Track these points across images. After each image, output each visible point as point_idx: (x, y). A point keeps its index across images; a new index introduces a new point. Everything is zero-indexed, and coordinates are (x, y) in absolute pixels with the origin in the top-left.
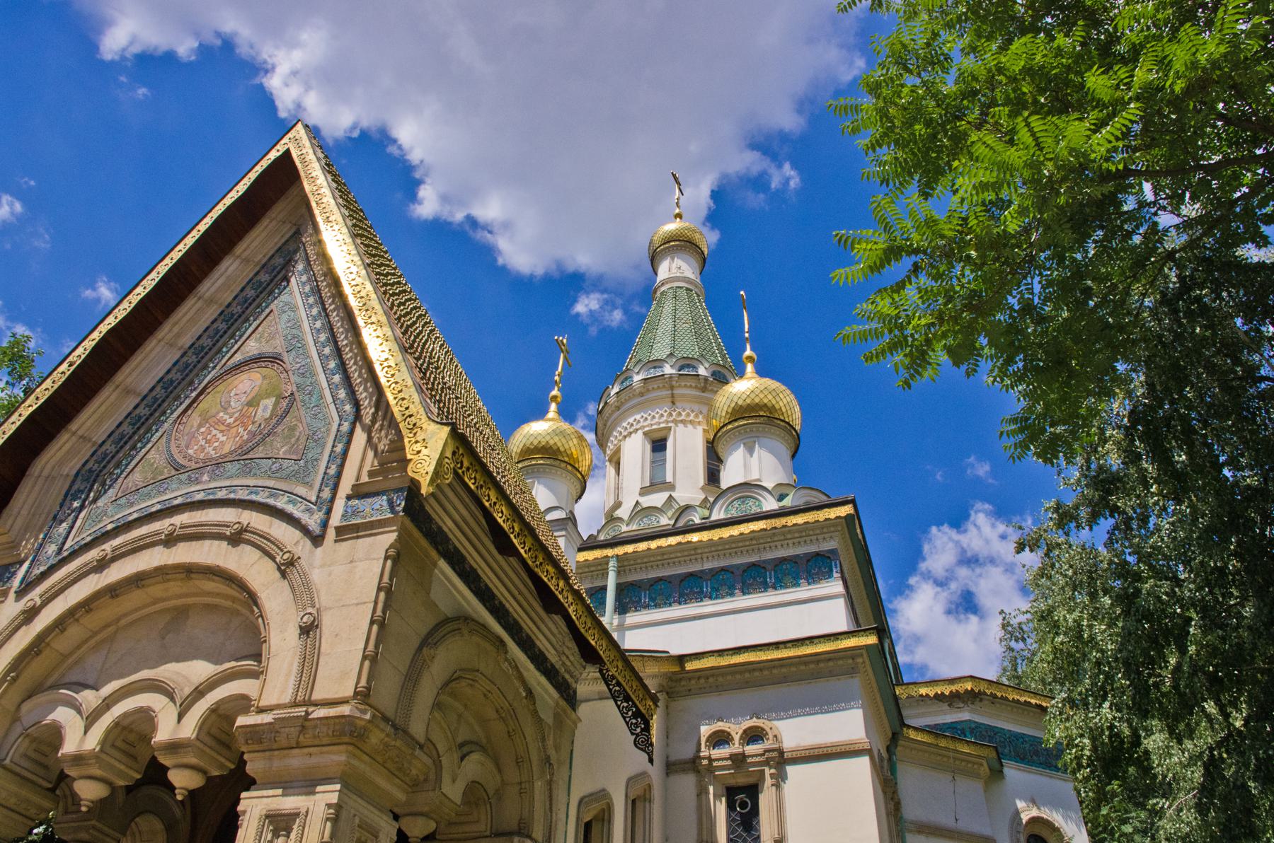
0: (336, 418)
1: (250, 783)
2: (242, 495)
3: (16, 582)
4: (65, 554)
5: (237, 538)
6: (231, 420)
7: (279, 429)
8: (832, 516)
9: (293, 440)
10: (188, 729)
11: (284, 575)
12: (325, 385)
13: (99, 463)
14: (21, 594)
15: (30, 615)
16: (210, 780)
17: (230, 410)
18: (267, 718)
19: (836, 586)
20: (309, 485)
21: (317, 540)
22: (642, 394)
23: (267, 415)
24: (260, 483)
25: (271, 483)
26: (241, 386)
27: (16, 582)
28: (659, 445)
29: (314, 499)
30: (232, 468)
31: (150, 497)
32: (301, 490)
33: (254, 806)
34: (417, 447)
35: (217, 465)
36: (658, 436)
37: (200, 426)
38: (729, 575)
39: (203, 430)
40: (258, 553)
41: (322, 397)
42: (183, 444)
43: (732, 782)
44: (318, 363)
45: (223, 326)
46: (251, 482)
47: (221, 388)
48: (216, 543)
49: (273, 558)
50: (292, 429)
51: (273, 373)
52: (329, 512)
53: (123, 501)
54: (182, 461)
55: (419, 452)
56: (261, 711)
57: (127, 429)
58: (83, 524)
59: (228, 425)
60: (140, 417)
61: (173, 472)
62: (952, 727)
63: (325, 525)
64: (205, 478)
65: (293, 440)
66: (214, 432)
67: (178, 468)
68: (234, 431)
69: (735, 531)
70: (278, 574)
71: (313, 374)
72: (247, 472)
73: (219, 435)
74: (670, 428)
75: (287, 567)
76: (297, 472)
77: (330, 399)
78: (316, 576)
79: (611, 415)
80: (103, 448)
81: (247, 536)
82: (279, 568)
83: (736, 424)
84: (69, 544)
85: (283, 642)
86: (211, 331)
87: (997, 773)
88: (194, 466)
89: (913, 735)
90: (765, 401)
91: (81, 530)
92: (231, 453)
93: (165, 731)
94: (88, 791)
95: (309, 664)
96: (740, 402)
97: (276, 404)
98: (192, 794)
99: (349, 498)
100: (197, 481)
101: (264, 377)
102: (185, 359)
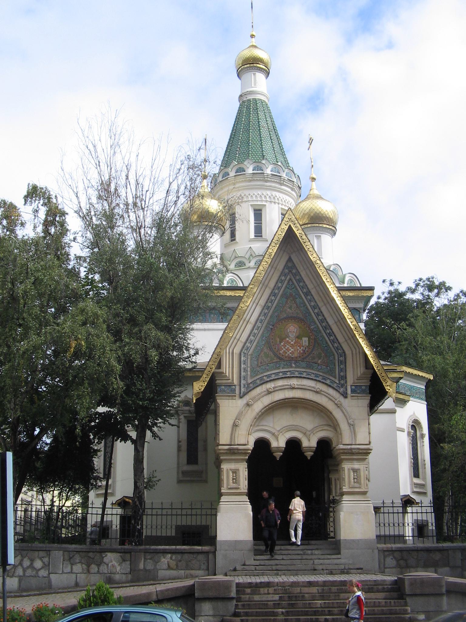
0: (336, 354)
2: (312, 376)
3: (237, 392)
6: (292, 343)
8: (365, 295)
9: (322, 358)
10: (313, 443)
14: (241, 397)
18: (349, 447)
20: (335, 377)
22: (250, 181)
23: (307, 344)
25: (321, 374)
26: (290, 328)
27: (237, 392)
28: (258, 214)
29: (338, 382)
30: (304, 364)
31: (275, 369)
32: (333, 379)
37: (280, 342)
39: (282, 344)
41: (327, 343)
44: (321, 328)
48: (311, 393)
49: (334, 402)
56: (344, 445)
57: (252, 338)
60: (255, 334)
61: (278, 360)
63: (347, 393)
65: (322, 358)
67: (281, 359)
71: (320, 332)
72: (309, 366)
74: (265, 205)
75: (338, 406)
78: (349, 409)
81: (322, 393)
82: (336, 404)
85: (344, 426)
91: (252, 377)
92: (300, 357)
97: (309, 341)
99: (351, 386)
100: (292, 367)
101: (300, 327)
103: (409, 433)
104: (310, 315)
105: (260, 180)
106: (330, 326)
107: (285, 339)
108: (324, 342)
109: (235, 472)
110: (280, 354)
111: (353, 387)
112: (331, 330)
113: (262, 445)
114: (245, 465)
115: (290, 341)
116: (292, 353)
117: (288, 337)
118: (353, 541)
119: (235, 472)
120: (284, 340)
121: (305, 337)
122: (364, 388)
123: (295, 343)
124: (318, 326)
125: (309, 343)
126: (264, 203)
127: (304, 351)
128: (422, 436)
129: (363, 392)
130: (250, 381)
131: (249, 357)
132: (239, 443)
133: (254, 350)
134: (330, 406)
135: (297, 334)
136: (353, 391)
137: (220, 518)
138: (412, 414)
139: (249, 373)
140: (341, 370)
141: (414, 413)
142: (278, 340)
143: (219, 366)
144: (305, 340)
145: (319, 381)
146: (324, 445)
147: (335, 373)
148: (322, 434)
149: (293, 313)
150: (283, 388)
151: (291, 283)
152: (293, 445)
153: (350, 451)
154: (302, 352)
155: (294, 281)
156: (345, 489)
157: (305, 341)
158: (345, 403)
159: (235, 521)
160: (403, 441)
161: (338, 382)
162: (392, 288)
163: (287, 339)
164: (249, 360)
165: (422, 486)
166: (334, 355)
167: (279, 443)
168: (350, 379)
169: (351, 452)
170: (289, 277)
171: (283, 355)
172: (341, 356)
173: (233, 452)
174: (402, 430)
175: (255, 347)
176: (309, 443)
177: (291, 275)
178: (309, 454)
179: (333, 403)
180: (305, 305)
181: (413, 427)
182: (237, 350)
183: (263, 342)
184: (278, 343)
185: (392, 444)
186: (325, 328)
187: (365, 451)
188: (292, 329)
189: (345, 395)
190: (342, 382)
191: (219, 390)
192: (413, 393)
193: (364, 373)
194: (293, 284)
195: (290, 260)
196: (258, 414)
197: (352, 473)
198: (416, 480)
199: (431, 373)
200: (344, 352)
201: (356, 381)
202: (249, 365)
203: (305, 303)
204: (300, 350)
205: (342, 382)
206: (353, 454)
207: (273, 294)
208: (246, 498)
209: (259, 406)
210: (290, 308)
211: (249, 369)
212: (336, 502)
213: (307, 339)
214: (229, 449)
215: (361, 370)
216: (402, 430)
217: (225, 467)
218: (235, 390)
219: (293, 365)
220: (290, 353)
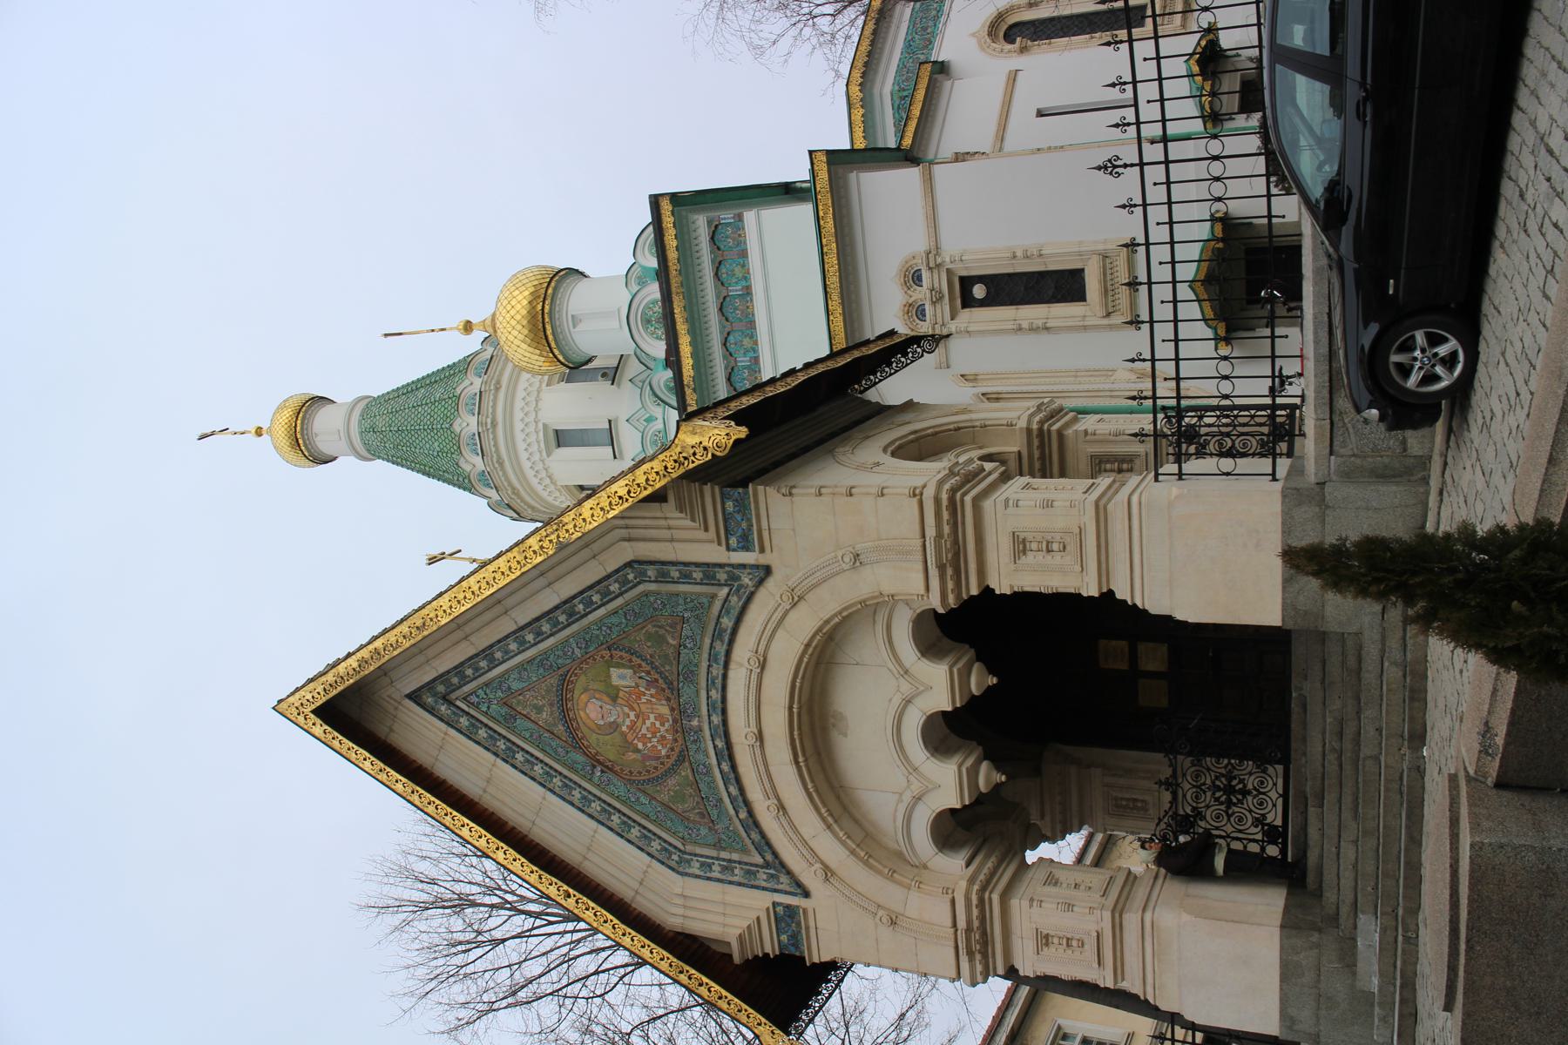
0: (641, 588)
1: (987, 591)
2: (717, 671)
4: (769, 857)
6: (632, 715)
7: (648, 652)
9: (662, 632)
11: (801, 598)
12: (602, 612)
13: (671, 854)
14: (807, 894)
15: (828, 873)
16: (978, 659)
17: (620, 720)
19: (750, 216)
20: (714, 596)
21: (768, 570)
23: (629, 672)
24: (705, 656)
25: (707, 641)
26: (593, 715)
28: (561, 438)
29: (726, 590)
30: (687, 691)
31: (714, 781)
33: (1004, 581)
34: (700, 451)
35: (681, 714)
36: (552, 436)
38: (731, 338)
39: (640, 746)
40: (780, 633)
42: (654, 763)
43: (959, 302)
44: (575, 627)
45: (519, 756)
46: (705, 664)
47: (593, 738)
50: (649, 636)
51: (583, 678)
52: (744, 566)
53: (714, 813)
54: (674, 758)
55: (705, 449)
57: (635, 832)
58: (736, 851)
59: (637, 716)
62: (896, 109)
63: (757, 567)
64: (695, 723)
65: (662, 632)
66: (644, 731)
67: (682, 758)
68: (643, 708)
69: (682, 328)
70: (802, 605)
71: (587, 629)
72: (690, 676)
73: (648, 723)
74: (545, 426)
76: (697, 617)
77: (620, 601)
79: (523, 500)
80: (656, 854)
81: (761, 649)
83: (551, 338)
84: (759, 860)
86: (526, 768)
87: (942, 68)
88: (681, 741)
89: (907, 142)
90: (525, 302)
91: (744, 851)
92: (668, 699)
94: (988, 776)
96: (526, 332)
97: (618, 666)
98: (992, 671)
99: (728, 548)
101: (586, 690)
102: (557, 790)
103: (1023, 50)
104: (545, 654)
105: (495, 438)
106: (565, 602)
107: (624, 735)
108: (614, 620)
109: (1044, 940)
110: (668, 757)
111: (733, 541)
112: (574, 597)
113: (955, 829)
115: (628, 722)
116: (659, 717)
117: (614, 726)
120: (630, 737)
121: (609, 676)
122: (730, 505)
123: (632, 709)
124: (573, 635)
125: (624, 666)
126: (540, 426)
127: (650, 684)
129: (742, 506)
130: (759, 860)
131: (689, 848)
132: (949, 922)
133: (668, 830)
135: (606, 699)
136: (746, 545)
138: (974, 41)
139: (735, 856)
140: (686, 577)
141: (973, 35)
142: (632, 756)
144: (621, 677)
145: (728, 653)
147: (699, 594)
149: (551, 705)
151: (474, 699)
153: (949, 571)
154: (653, 691)
155: (467, 688)
156: (1091, 590)
157: (622, 677)
161: (726, 590)
163: (624, 728)
164: (698, 850)
166: (647, 594)
167: (946, 782)
168: (714, 553)
170: (458, 703)
171: (672, 749)
172: (644, 573)
174: (1013, 77)
175: (660, 826)
176: (938, 685)
177: (453, 696)
178: (979, 681)
179: (792, 615)
180: (521, 667)
181: (1009, 37)
183: (643, 800)
184: (638, 756)
186: (573, 617)
187: (946, 515)
190: (722, 576)
191: (792, 950)
193: (681, 509)
194: (474, 693)
195: (414, 696)
196: (853, 852)
197: (1030, 558)
200: (629, 564)
201: (712, 533)
202: (714, 853)
203: (517, 666)
205: (722, 576)
206: (957, 555)
209: (830, 848)
210: (539, 710)
211: (724, 855)
213: (614, 672)
214: (970, 954)
216: (1013, 77)
218: (788, 907)
219: (695, 723)
220: (662, 724)
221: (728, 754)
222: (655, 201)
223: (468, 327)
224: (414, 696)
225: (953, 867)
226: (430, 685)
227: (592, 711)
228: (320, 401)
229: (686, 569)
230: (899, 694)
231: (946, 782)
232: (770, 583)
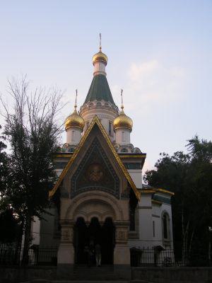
5: (106, 197)
33: (118, 231)
75: (115, 203)
87: (161, 205)
93: (100, 220)
95: (122, 215)
109: (67, 232)
113: (81, 220)
114: (72, 229)
118: (120, 265)
119: (67, 232)
128: (169, 220)
134: (111, 203)
137: (59, 253)
143: (62, 183)
144: (101, 173)
146: (109, 220)
148: (107, 216)
150: (90, 195)
152: (95, 220)
158: (118, 201)
159: (66, 255)
160: (159, 222)
162: (164, 157)
165: (169, 242)
167: (88, 219)
169: (120, 224)
173: (66, 223)
176: (102, 220)
178: (102, 225)
181: (165, 216)
182: (70, 178)
185: (153, 221)
188: (96, 168)
189: (119, 199)
192: (166, 201)
198: (165, 240)
199: (172, 191)
204: (99, 178)
207: (88, 152)
208: (71, 244)
209: (78, 203)
212: (114, 246)
215: (126, 186)
217: (63, 230)
221: (91, 189)
222: (145, 154)
223: (122, 108)
224: (96, 138)
225: (76, 220)
226: (98, 141)
227: (96, 168)
228: (106, 64)
229: (118, 187)
230: (101, 214)
231: (88, 219)
232: (117, 200)
